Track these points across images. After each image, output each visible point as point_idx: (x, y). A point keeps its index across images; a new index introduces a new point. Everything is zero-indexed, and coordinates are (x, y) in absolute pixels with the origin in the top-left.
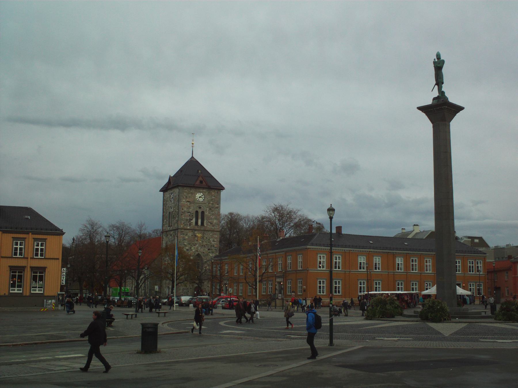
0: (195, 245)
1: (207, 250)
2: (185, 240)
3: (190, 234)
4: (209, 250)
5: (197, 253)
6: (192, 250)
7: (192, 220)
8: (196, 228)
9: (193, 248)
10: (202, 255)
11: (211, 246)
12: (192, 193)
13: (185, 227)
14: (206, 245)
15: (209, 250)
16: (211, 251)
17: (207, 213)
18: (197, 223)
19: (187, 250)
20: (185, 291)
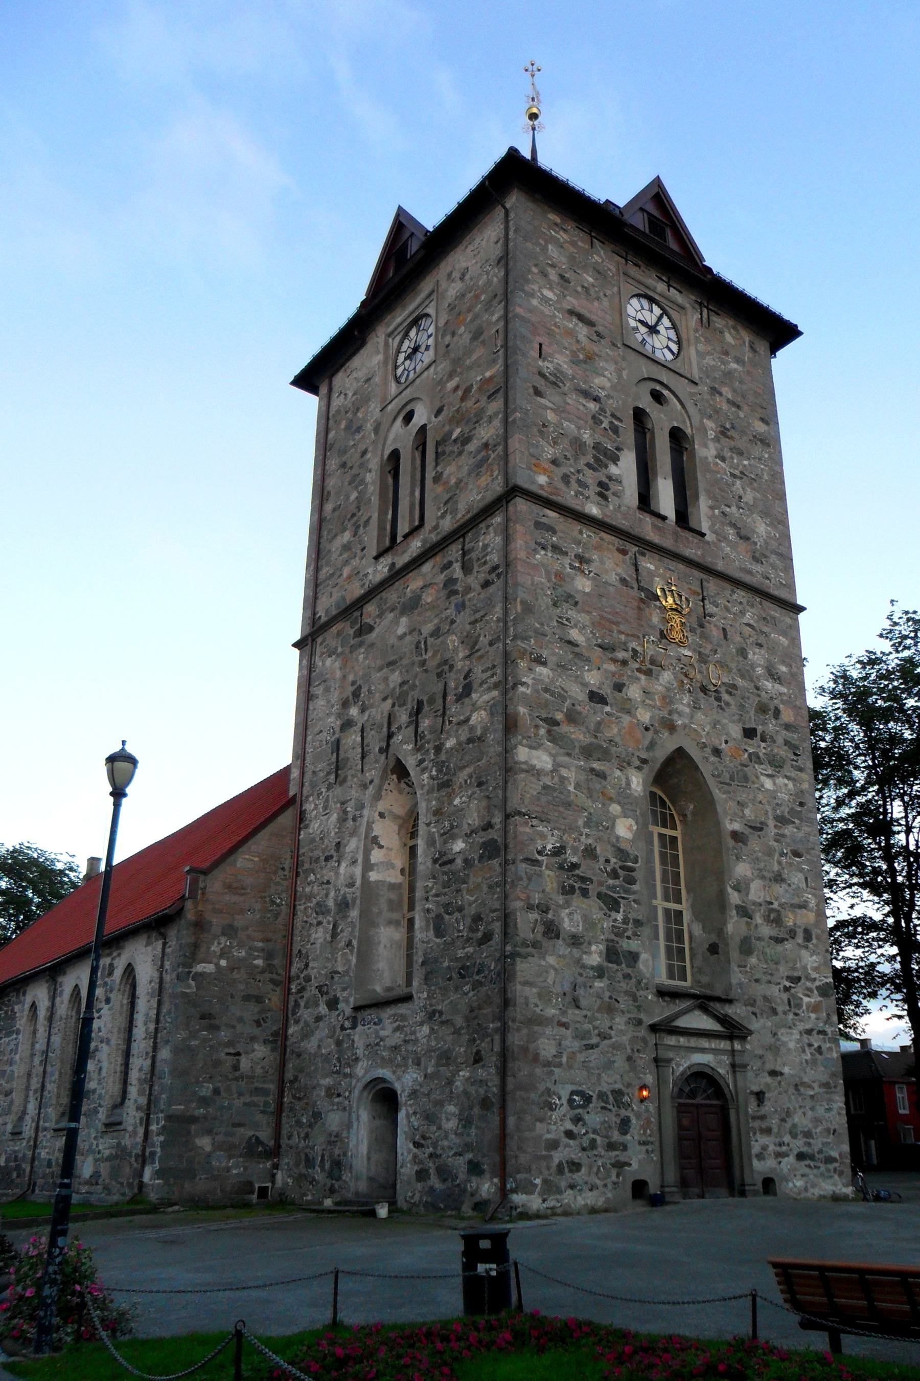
0: (651, 668)
1: (736, 731)
2: (570, 599)
3: (610, 564)
4: (749, 733)
5: (668, 744)
6: (627, 708)
7: (615, 460)
8: (647, 528)
9: (634, 692)
10: (707, 767)
11: (762, 709)
12: (599, 272)
13: (569, 497)
14: (732, 688)
15: (749, 733)
16: (762, 749)
17: (706, 451)
18: (645, 500)
19: (596, 697)
20: (594, 1118)
